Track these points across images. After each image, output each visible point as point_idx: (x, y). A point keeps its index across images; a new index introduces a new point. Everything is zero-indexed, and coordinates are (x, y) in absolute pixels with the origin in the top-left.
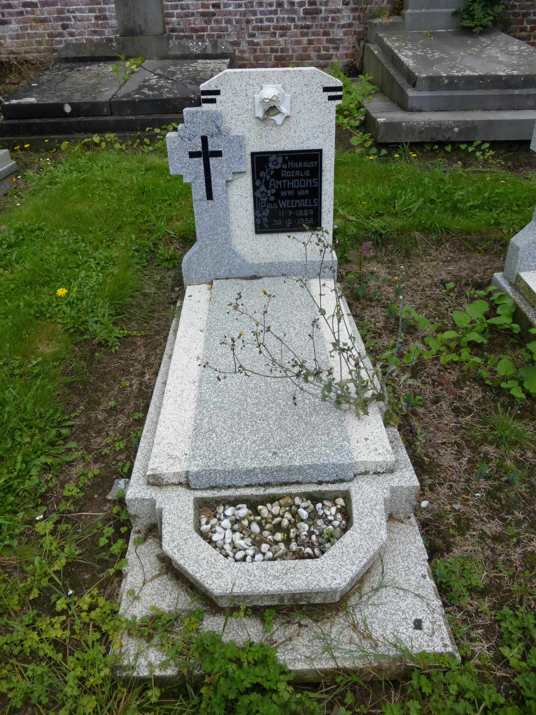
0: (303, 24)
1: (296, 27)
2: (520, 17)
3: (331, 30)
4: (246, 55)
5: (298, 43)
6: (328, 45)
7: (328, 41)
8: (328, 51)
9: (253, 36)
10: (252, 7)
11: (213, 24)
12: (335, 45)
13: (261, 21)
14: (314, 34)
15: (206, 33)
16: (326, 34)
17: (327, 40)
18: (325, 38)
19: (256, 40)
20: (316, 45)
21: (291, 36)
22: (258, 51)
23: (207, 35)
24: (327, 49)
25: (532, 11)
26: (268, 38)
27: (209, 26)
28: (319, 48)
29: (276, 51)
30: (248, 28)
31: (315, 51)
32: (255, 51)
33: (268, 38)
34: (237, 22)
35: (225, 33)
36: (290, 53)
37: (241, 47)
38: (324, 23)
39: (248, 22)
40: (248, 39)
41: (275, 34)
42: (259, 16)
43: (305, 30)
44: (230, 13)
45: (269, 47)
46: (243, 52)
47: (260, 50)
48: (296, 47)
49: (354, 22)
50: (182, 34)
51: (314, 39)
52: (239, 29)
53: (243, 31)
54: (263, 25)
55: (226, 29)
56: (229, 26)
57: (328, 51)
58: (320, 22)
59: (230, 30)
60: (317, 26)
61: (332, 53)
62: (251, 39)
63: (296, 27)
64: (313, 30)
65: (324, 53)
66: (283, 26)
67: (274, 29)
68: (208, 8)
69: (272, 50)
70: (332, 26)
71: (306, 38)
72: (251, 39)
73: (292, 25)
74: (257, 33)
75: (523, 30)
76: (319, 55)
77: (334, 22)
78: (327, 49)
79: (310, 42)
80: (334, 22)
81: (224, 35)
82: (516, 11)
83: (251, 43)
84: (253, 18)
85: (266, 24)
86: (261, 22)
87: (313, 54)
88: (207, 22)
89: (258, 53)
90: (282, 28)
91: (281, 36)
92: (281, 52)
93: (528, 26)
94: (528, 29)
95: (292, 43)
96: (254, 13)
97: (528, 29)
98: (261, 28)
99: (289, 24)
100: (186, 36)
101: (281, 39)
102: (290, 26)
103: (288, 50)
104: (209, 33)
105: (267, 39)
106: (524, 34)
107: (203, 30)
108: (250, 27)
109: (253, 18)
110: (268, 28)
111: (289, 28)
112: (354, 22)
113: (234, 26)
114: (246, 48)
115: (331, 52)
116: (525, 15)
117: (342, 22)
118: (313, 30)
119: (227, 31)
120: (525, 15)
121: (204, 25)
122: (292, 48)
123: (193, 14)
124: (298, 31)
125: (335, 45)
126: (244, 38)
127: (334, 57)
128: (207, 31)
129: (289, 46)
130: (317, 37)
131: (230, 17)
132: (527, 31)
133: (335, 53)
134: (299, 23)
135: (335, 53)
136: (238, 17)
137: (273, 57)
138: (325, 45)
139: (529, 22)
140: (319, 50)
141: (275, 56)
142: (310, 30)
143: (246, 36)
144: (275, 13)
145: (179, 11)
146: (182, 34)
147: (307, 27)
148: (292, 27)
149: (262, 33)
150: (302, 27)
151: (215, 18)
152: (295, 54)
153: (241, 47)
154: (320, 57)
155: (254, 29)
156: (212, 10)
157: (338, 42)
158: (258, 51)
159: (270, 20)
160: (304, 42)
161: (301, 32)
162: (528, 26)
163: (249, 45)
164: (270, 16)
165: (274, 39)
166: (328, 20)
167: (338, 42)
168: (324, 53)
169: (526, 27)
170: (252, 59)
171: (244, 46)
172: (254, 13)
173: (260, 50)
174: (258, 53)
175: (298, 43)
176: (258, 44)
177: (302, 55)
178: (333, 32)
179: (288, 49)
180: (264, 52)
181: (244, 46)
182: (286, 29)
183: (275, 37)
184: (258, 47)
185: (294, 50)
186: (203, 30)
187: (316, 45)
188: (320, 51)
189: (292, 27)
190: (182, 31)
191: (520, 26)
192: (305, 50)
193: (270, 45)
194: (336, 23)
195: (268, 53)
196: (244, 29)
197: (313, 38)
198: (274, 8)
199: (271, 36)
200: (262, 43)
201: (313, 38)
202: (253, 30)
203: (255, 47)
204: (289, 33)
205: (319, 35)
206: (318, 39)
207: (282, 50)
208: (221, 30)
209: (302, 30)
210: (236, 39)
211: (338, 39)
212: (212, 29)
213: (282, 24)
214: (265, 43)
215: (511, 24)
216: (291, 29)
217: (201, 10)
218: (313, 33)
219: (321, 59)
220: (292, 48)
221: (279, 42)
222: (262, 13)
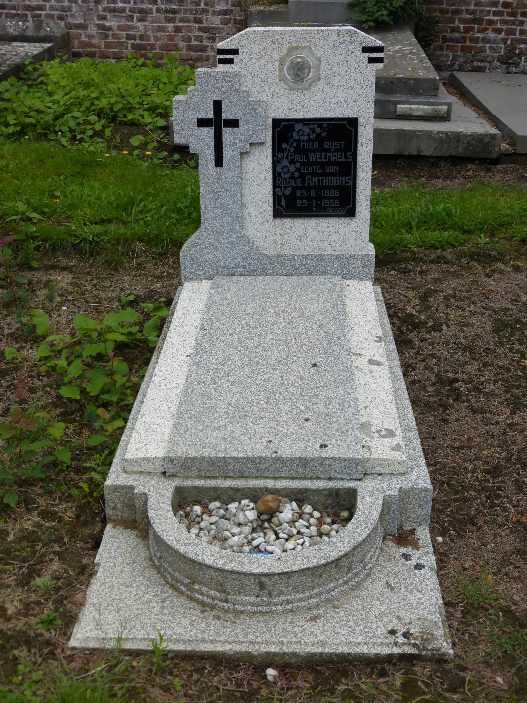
0: (168, 8)
1: (158, 10)
2: (450, 15)
3: (205, 17)
4: (95, 41)
5: (162, 29)
6: (201, 34)
7: (200, 29)
8: (201, 42)
9: (104, 18)
12: (211, 35)
14: (182, 20)
15: (44, 12)
16: (197, 21)
17: (199, 27)
18: (197, 25)
19: (107, 24)
20: (184, 33)
21: (153, 22)
22: (110, 37)
23: (45, 15)
24: (199, 39)
25: (463, 8)
27: (48, 5)
28: (190, 37)
29: (134, 38)
30: (97, 9)
31: (183, 41)
32: (107, 36)
35: (68, 13)
36: (152, 41)
37: (89, 32)
38: (194, 8)
40: (97, 22)
41: (131, 18)
43: (171, 15)
45: (124, 33)
46: (91, 37)
47: (113, 35)
48: (159, 34)
49: (233, 8)
50: (14, 12)
51: (182, 27)
52: (85, 10)
53: (91, 12)
54: (116, 6)
55: (70, 9)
56: (73, 5)
57: (201, 42)
58: (190, 7)
59: (74, 10)
60: (186, 10)
61: (206, 44)
62: (101, 22)
63: (158, 10)
64: (181, 15)
65: (196, 43)
66: (143, 9)
67: (130, 11)
69: (129, 37)
70: (205, 12)
71: (172, 25)
72: (101, 22)
73: (154, 8)
74: (108, 15)
75: (456, 30)
76: (189, 45)
77: (207, 8)
78: (199, 39)
79: (177, 30)
80: (207, 8)
81: (67, 16)
82: (444, 6)
83: (99, 27)
86: (114, 3)
87: (182, 44)
89: (110, 39)
90: (141, 11)
91: (140, 20)
92: (140, 40)
93: (461, 26)
94: (462, 30)
95: (153, 30)
97: (462, 30)
98: (114, 10)
99: (150, 6)
100: (18, 15)
102: (151, 10)
103: (148, 38)
104: (48, 12)
105: (122, 23)
106: (457, 35)
108: (100, 8)
110: (123, 10)
111: (150, 12)
112: (233, 8)
113: (79, 5)
114: (94, 33)
115: (205, 43)
116: (456, 12)
117: (218, 8)
118: (181, 15)
119: (71, 11)
120: (456, 12)
122: (154, 36)
124: (162, 16)
125: (211, 35)
126: (92, 20)
127: (209, 49)
128: (45, 10)
129: (150, 33)
130: (186, 24)
132: (460, 32)
133: (210, 44)
134: (163, 7)
135: (210, 44)
137: (129, 45)
138: (197, 33)
139: (462, 21)
140: (189, 39)
141: (133, 45)
142: (177, 15)
143: (95, 18)
146: (14, 12)
147: (174, 12)
148: (154, 11)
149: (115, 16)
150: (166, 11)
152: (158, 43)
153: (89, 32)
154: (190, 48)
155: (104, 10)
157: (214, 32)
158: (110, 37)
160: (170, 29)
161: (166, 17)
162: (461, 26)
163: (99, 29)
165: (131, 23)
166: (200, 5)
167: (214, 32)
168: (196, 43)
169: (459, 27)
170: (103, 46)
171: (92, 30)
173: (113, 35)
174: (110, 39)
175: (162, 29)
176: (110, 28)
177: (167, 44)
178: (207, 18)
179: (149, 36)
180: (119, 39)
181: (92, 30)
182: (146, 13)
183: (132, 21)
184: (111, 33)
185: (156, 38)
187: (184, 33)
188: (190, 41)
189: (154, 11)
190: (14, 8)
191: (451, 25)
192: (171, 38)
193: (125, 30)
194: (211, 9)
195: (124, 40)
196: (91, 10)
197: (181, 24)
199: (127, 20)
200: (115, 28)
201: (181, 24)
202: (104, 11)
203: (107, 32)
204: (150, 17)
205: (188, 22)
206: (188, 26)
207: (141, 37)
208: (63, 9)
209: (166, 15)
210: (82, 21)
211: (213, 28)
212: (52, 8)
213: (141, 7)
214: (119, 28)
215: (438, 22)
216: (152, 13)
218: (180, 18)
219: (193, 51)
220: (154, 36)
221: (137, 27)
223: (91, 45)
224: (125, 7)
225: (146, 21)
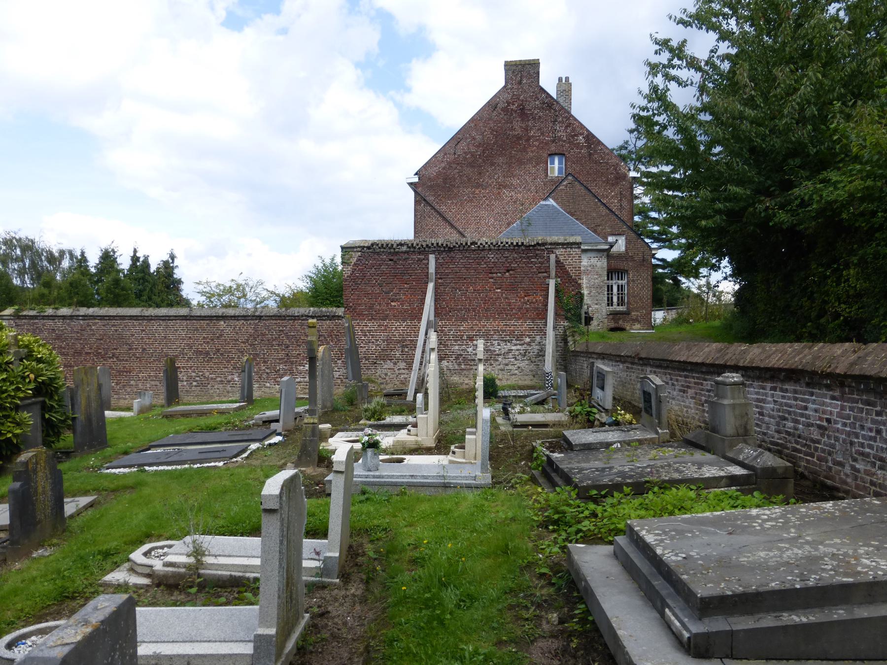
4: (849, 480)
9: (855, 460)
10: (855, 429)
11: (826, 439)
13: (862, 445)
19: (857, 466)
26: (869, 468)
30: (851, 450)
33: (869, 468)
34: (844, 440)
39: (852, 443)
42: (861, 440)
44: (838, 430)
45: (869, 478)
46: (847, 475)
59: (837, 448)
67: (873, 458)
68: (823, 421)
74: (860, 458)
84: (856, 440)
85: (867, 450)
88: (822, 435)
91: (881, 468)
96: (857, 436)
98: (862, 454)
101: (879, 472)
107: (819, 442)
109: (856, 440)
110: (867, 455)
121: (819, 437)
123: (812, 425)
131: (837, 434)
136: (844, 436)
144: (874, 439)
145: (804, 419)
151: (827, 432)
156: (825, 424)
159: (871, 447)
164: (871, 443)
171: (847, 469)
172: (857, 436)
176: (858, 471)
180: (864, 482)
181: (847, 469)
186: (819, 442)
190: (804, 439)
195: (868, 485)
198: (873, 434)
200: (862, 471)
213: (882, 455)
217: (818, 422)
222: (864, 437)
223: (846, 483)
224: (870, 453)
225: (884, 470)
